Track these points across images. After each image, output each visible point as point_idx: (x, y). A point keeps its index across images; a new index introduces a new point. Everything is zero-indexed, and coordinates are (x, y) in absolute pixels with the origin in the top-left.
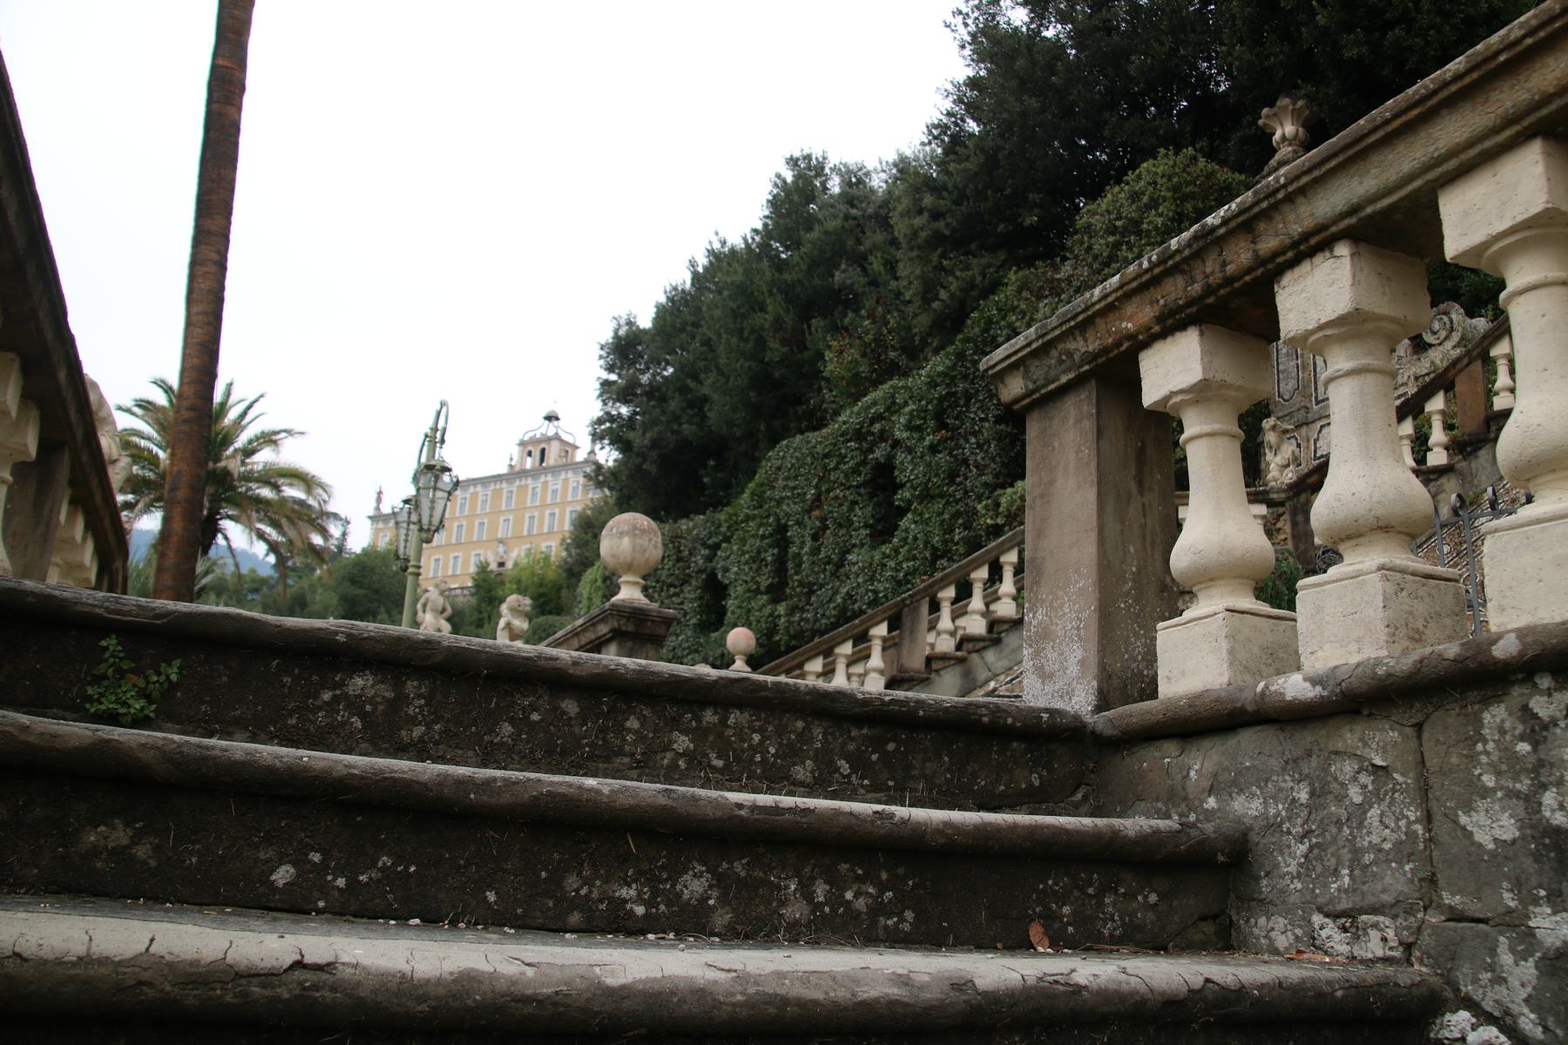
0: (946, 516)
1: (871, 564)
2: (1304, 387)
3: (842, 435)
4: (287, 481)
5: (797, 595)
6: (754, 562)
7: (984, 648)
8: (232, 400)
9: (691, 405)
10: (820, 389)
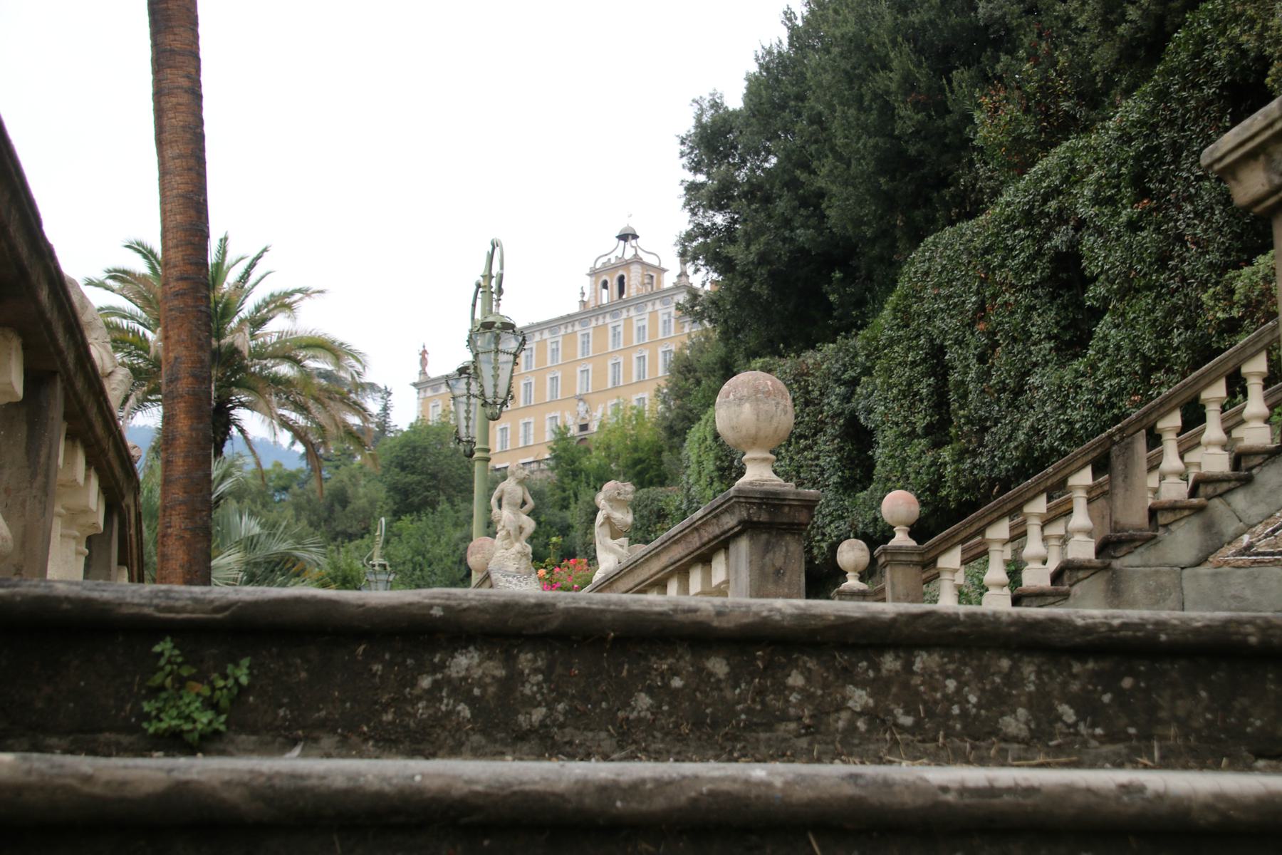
0: (1159, 314)
1: (1060, 387)
3: (1006, 222)
4: (310, 353)
5: (965, 435)
6: (905, 397)
7: (1230, 491)
8: (230, 258)
9: (804, 203)
10: (971, 163)
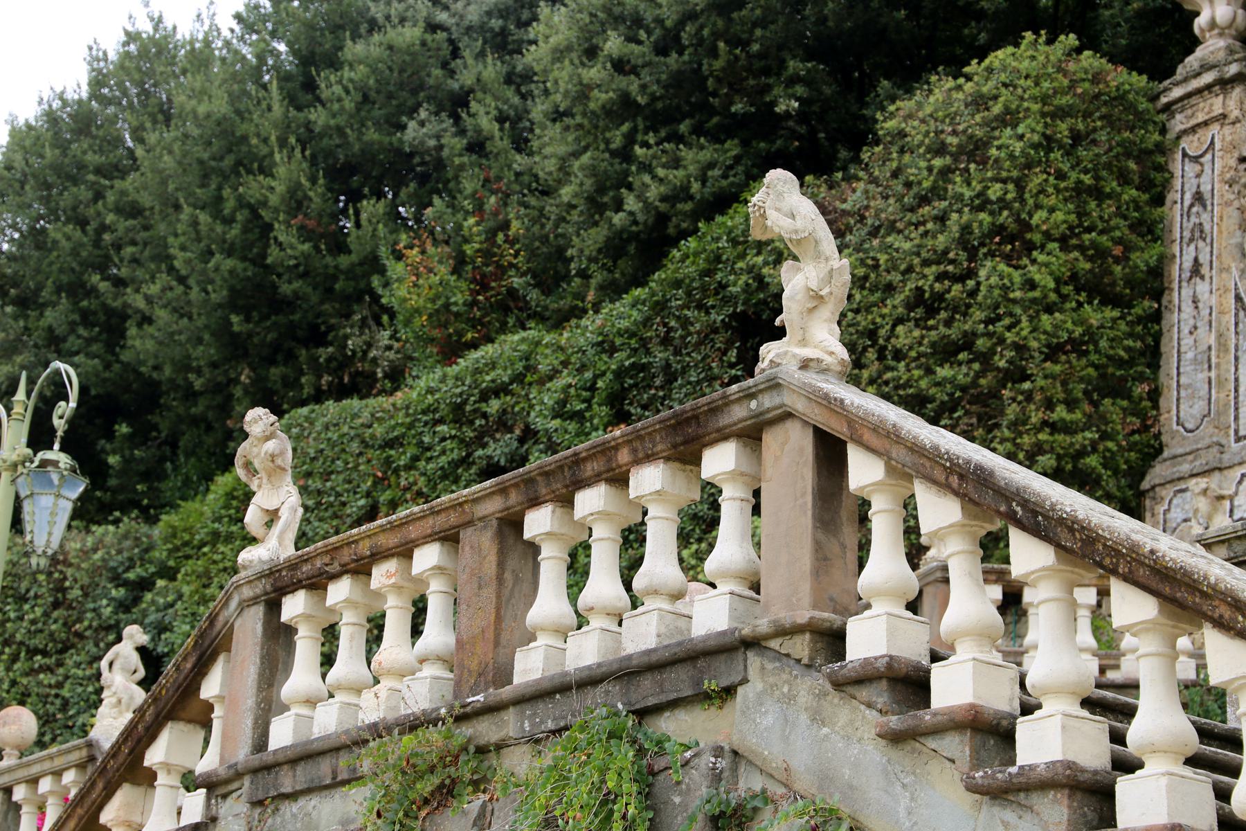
2: (1218, 414)
9: (86, 318)
